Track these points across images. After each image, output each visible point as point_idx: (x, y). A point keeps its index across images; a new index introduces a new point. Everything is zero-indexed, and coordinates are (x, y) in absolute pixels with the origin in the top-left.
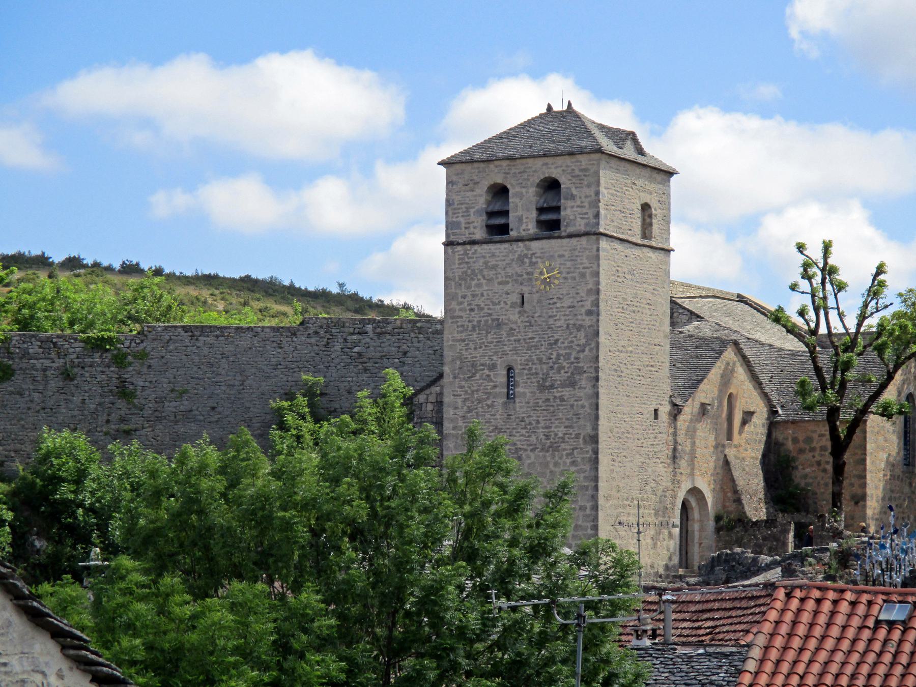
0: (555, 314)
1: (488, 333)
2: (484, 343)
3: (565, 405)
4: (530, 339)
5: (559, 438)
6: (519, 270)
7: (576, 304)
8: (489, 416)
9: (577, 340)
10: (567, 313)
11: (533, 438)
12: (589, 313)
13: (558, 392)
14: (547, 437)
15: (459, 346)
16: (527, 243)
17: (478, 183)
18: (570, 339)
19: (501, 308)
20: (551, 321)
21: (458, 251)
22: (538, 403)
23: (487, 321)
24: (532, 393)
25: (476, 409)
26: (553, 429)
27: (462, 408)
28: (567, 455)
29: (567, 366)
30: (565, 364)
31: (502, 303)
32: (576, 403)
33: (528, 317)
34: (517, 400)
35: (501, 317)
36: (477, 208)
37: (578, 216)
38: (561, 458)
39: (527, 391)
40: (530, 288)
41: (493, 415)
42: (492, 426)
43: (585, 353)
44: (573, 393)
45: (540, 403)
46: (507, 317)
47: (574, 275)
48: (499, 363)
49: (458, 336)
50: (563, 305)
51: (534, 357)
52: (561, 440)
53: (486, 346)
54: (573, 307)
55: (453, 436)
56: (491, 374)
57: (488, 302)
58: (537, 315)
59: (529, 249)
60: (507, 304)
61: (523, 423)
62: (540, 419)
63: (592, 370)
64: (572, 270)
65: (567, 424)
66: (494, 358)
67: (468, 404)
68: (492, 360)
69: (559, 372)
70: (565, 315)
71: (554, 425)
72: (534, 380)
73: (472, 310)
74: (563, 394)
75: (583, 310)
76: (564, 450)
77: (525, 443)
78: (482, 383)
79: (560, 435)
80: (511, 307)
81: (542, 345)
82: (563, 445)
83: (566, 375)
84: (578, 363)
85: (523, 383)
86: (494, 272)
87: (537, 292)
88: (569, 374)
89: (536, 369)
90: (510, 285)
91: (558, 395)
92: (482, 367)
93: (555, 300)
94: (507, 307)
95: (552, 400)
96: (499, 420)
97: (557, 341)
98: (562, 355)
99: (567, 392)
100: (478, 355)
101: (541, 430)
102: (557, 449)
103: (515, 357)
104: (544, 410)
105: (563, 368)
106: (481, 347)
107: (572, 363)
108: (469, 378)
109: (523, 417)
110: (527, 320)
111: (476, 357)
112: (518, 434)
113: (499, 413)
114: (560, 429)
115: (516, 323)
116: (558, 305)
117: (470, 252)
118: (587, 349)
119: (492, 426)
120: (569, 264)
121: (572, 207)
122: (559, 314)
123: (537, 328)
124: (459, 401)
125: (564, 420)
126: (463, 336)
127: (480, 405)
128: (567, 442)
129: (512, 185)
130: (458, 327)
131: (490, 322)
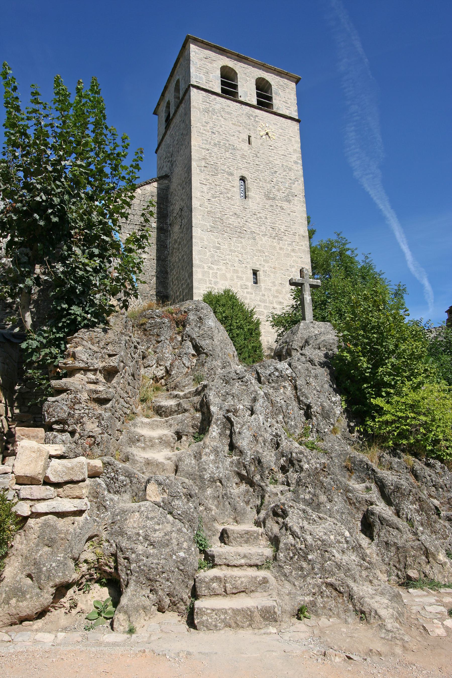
1: (226, 151)
2: (223, 156)
4: (257, 165)
6: (247, 122)
11: (263, 228)
13: (279, 203)
15: (204, 152)
20: (271, 159)
28: (289, 244)
30: (282, 187)
35: (236, 145)
38: (284, 245)
42: (232, 212)
51: (261, 178)
52: (283, 234)
56: (230, 178)
58: (261, 152)
69: (278, 191)
72: (262, 191)
76: (286, 241)
77: (258, 229)
82: (285, 237)
88: (285, 194)
90: (241, 128)
91: (279, 205)
94: (240, 140)
96: (237, 209)
99: (285, 205)
102: (281, 239)
106: (221, 159)
107: (287, 188)
112: (252, 222)
116: (275, 151)
118: (296, 183)
119: (232, 212)
120: (281, 131)
124: (205, 189)
126: (207, 147)
131: (227, 145)
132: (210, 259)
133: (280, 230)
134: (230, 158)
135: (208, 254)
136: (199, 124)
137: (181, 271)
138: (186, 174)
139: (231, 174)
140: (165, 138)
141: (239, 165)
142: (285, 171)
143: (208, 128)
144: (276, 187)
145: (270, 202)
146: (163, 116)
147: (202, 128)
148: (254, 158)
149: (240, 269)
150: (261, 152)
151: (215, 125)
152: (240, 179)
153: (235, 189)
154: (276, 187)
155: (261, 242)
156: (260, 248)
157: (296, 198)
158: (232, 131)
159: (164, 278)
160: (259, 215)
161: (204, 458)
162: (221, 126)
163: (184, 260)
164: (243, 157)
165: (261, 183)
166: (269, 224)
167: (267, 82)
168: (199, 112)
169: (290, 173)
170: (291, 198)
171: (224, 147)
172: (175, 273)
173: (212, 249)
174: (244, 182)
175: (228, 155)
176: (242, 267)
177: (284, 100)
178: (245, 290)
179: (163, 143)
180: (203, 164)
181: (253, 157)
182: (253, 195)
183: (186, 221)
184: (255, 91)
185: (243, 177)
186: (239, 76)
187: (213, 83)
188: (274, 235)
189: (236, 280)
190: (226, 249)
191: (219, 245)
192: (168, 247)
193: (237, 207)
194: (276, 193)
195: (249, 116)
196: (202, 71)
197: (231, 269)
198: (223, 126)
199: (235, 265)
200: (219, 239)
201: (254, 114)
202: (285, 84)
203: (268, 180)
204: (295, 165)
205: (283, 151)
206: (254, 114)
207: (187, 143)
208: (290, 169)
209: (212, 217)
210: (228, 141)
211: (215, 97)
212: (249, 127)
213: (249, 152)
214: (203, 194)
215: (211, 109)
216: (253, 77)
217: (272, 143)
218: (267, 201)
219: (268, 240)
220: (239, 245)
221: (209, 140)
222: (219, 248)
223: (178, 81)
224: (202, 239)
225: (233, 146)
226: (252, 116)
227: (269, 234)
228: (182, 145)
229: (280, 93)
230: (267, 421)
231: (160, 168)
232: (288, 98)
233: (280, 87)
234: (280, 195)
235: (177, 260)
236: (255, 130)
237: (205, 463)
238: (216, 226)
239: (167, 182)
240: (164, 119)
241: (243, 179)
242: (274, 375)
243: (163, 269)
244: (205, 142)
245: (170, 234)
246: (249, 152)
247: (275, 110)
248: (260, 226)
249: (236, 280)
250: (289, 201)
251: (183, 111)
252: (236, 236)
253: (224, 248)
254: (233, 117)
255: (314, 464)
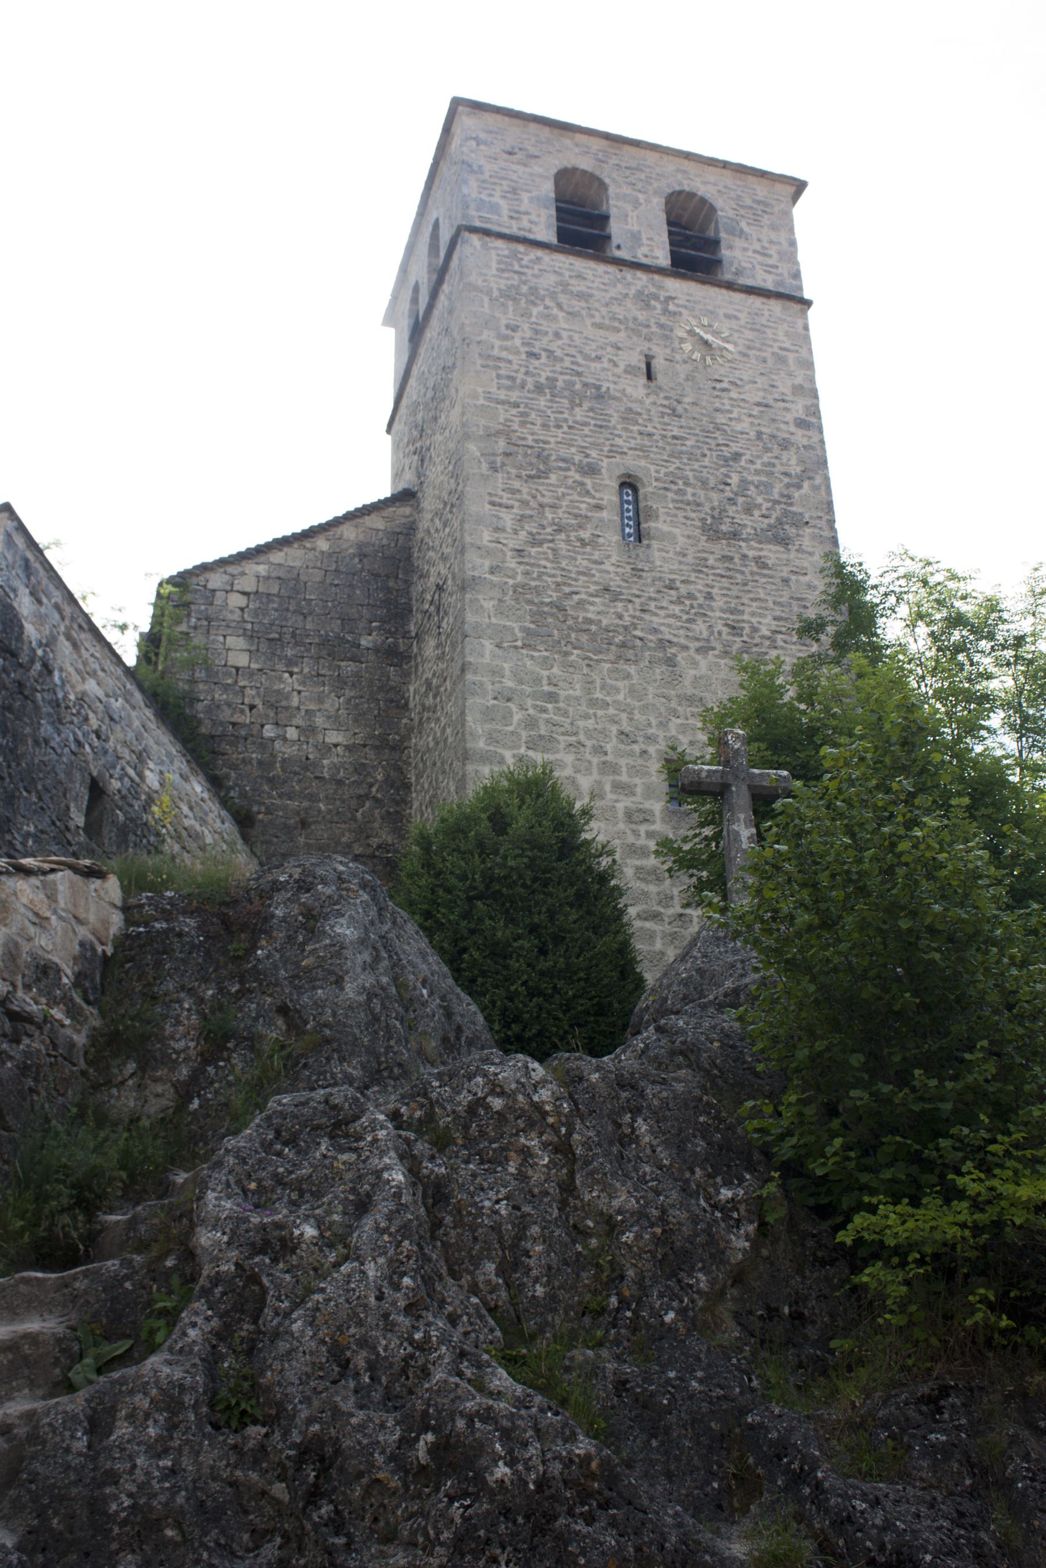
0: (728, 407)
1: (573, 405)
2: (566, 420)
3: (771, 577)
4: (674, 437)
5: (763, 637)
6: (642, 316)
7: (771, 402)
8: (585, 563)
9: (782, 464)
10: (754, 413)
11: (700, 627)
12: (801, 424)
13: (751, 548)
14: (735, 629)
16: (656, 277)
17: (536, 157)
18: (765, 459)
19: (604, 369)
20: (720, 419)
21: (496, 248)
22: (706, 560)
23: (570, 384)
24: (689, 537)
25: (552, 541)
26: (746, 617)
27: (516, 532)
29: (765, 505)
30: (759, 500)
31: (605, 360)
32: (793, 578)
33: (666, 398)
34: (655, 545)
36: (535, 193)
37: (758, 267)
39: (677, 531)
40: (668, 351)
41: (596, 562)
42: (596, 583)
43: (803, 491)
44: (785, 556)
45: (711, 562)
46: (619, 387)
47: (763, 354)
48: (604, 464)
49: (502, 395)
50: (742, 397)
51: (690, 474)
52: (767, 643)
53: (570, 427)
54: (766, 406)
55: (493, 585)
56: (588, 481)
57: (573, 351)
58: (687, 400)
59: (660, 287)
60: (616, 365)
61: (673, 592)
62: (715, 591)
63: (823, 524)
64: (758, 345)
65: (778, 613)
66: (594, 453)
67: (531, 527)
68: (587, 456)
69: (748, 511)
70: (750, 416)
71: (748, 610)
72: (693, 515)
73: (532, 355)
74: (762, 554)
75: (789, 417)
77: (682, 632)
78: (564, 495)
79: (765, 632)
80: (626, 372)
81: (705, 455)
83: (766, 521)
84: (791, 504)
85: (667, 514)
86: (583, 304)
87: (685, 362)
88: (772, 521)
89: (694, 495)
91: (751, 554)
92: (562, 465)
93: (725, 385)
95: (736, 560)
97: (737, 456)
98: (752, 483)
99: (772, 553)
100: (552, 440)
101: (718, 614)
103: (643, 463)
104: (722, 576)
105: (759, 506)
106: (559, 427)
107: (776, 502)
108: (530, 477)
109: (672, 581)
110: (666, 402)
111: (545, 442)
112: (662, 613)
113: (613, 560)
114: (764, 621)
115: (641, 402)
116: (733, 395)
117: (526, 258)
118: (806, 485)
119: (596, 583)
120: (749, 335)
121: (745, 249)
122: (736, 410)
123: (692, 424)
124: (508, 519)
125: (770, 605)
126: (515, 396)
127: (563, 536)
128: (782, 648)
129: (614, 181)
130: (499, 377)
131: (578, 386)
132: (524, 734)
133: (755, 630)
134: (586, 424)
135: (516, 718)
136: (486, 332)
137: (441, 778)
138: (452, 481)
139: (592, 470)
140: (408, 388)
141: (619, 441)
142: (767, 450)
143: (517, 342)
144: (741, 500)
145: (721, 548)
146: (406, 324)
147: (497, 343)
148: (666, 419)
149: (623, 762)
150: (687, 400)
151: (537, 332)
152: (623, 485)
153: (604, 514)
154: (741, 500)
155: (693, 672)
156: (690, 691)
157: (808, 530)
158: (594, 346)
159: (397, 803)
160: (684, 589)
161: (123, 1430)
162: (557, 335)
163: (446, 740)
164: (629, 416)
165: (690, 490)
166: (718, 614)
167: (703, 201)
168: (486, 299)
169: (785, 456)
170: (792, 531)
171: (566, 393)
172: (426, 786)
173: (529, 702)
174: (635, 490)
175: (579, 414)
176: (631, 754)
177: (757, 246)
178: (643, 829)
179: (405, 402)
180: (501, 445)
181: (663, 415)
182: (665, 528)
183: (451, 620)
184: (665, 227)
185: (629, 476)
186: (612, 190)
187: (533, 217)
188: (735, 648)
189: (610, 796)
190: (577, 699)
191: (552, 689)
192: (411, 705)
193: (612, 569)
194: (742, 518)
195: (644, 300)
196: (498, 188)
197: (595, 761)
198: (564, 334)
199: (609, 747)
200: (555, 670)
201: (663, 295)
202: (759, 202)
203: (712, 482)
204: (800, 432)
205: (761, 394)
206: (663, 295)
207: (453, 391)
208: (785, 445)
209: (530, 602)
210: (579, 374)
211: (539, 253)
212: (645, 331)
213: (648, 401)
214: (501, 536)
215: (524, 289)
216: (655, 192)
217: (722, 371)
218: (709, 546)
219: (717, 664)
220: (620, 684)
221: (520, 376)
222: (552, 697)
223: (436, 225)
224: (496, 672)
225: (598, 388)
226: (656, 297)
227: (719, 647)
228: (443, 400)
229: (746, 229)
230: (397, 1287)
231: (397, 475)
232: (771, 242)
233: (742, 212)
234: (750, 523)
235: (432, 745)
236: (667, 337)
237: (123, 1450)
238: (543, 631)
239: (407, 510)
240: (406, 335)
241: (629, 484)
242: (488, 1107)
243: (393, 774)
244: (508, 383)
245: (416, 667)
246: (648, 401)
247: (728, 277)
248: (689, 621)
249: (610, 796)
250: (784, 542)
251: (446, 303)
252: (611, 657)
253: (568, 698)
254: (597, 305)
255: (536, 1461)
